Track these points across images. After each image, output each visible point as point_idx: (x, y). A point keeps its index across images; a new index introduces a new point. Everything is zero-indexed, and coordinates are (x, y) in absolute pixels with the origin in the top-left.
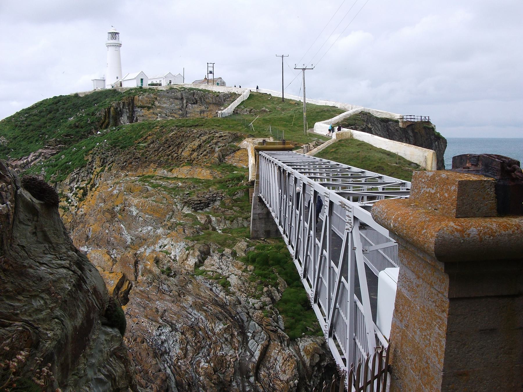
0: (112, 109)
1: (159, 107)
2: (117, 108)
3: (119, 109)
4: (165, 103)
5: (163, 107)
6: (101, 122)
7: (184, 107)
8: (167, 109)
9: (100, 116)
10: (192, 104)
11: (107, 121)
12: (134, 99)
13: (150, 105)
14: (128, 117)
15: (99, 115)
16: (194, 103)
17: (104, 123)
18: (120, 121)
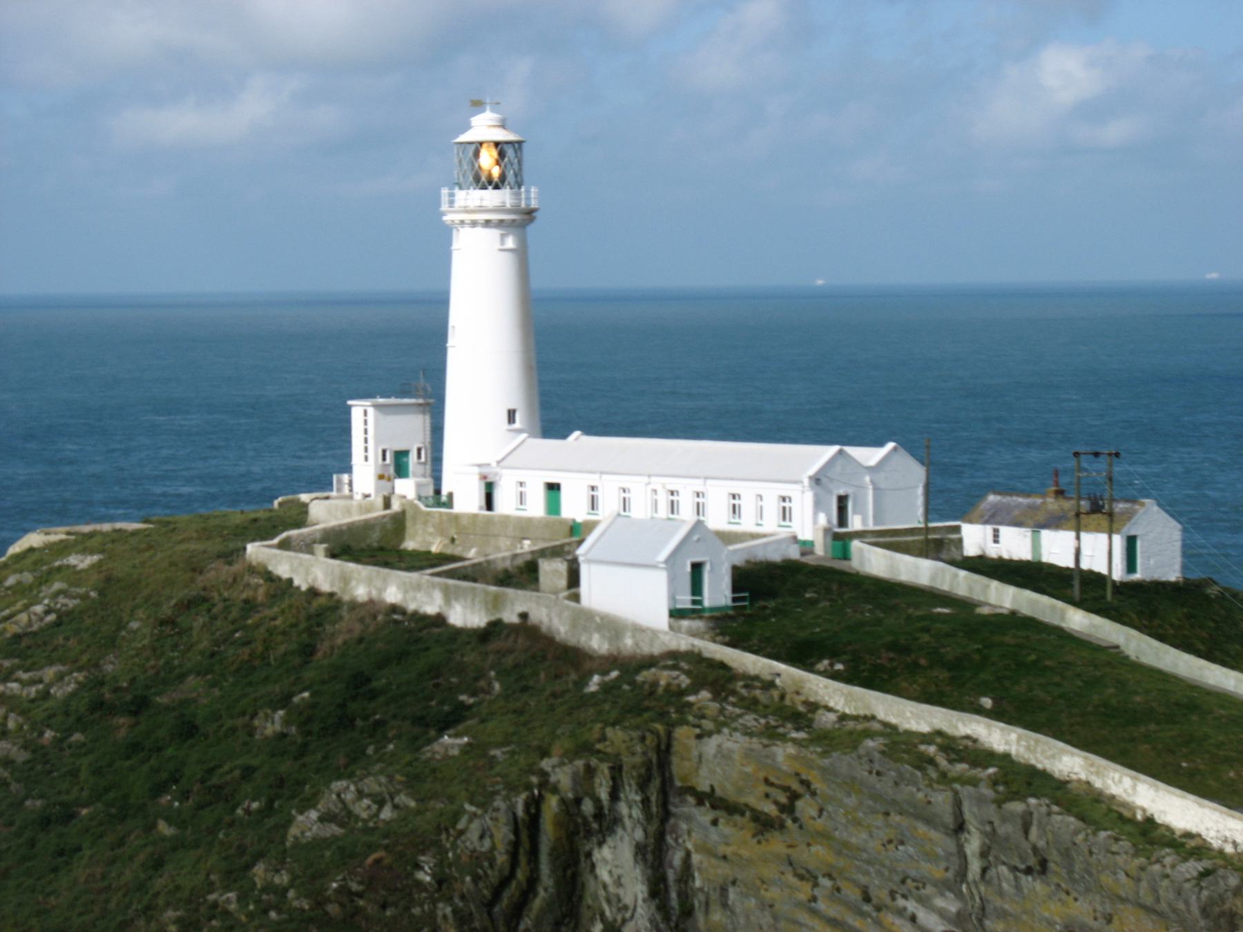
0: (552, 804)
1: (825, 836)
2: (578, 801)
3: (588, 807)
4: (857, 823)
5: (846, 844)
6: (494, 877)
7: (970, 876)
8: (869, 862)
9: (487, 843)
10: (1014, 869)
11: (521, 875)
12: (669, 746)
13: (770, 809)
14: (640, 850)
15: (482, 837)
16: (1029, 871)
17: (505, 882)
18: (593, 866)
